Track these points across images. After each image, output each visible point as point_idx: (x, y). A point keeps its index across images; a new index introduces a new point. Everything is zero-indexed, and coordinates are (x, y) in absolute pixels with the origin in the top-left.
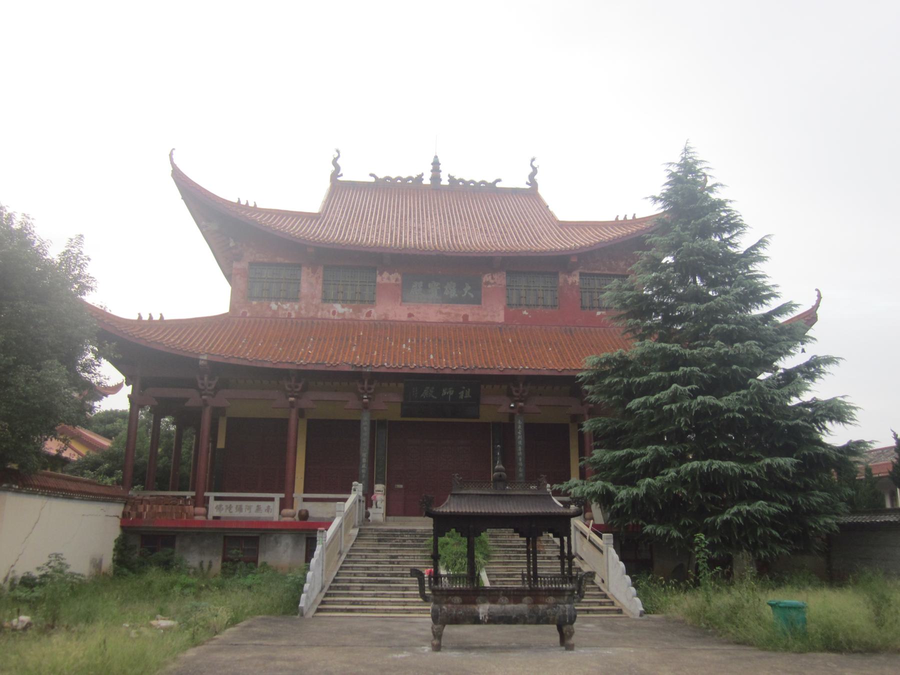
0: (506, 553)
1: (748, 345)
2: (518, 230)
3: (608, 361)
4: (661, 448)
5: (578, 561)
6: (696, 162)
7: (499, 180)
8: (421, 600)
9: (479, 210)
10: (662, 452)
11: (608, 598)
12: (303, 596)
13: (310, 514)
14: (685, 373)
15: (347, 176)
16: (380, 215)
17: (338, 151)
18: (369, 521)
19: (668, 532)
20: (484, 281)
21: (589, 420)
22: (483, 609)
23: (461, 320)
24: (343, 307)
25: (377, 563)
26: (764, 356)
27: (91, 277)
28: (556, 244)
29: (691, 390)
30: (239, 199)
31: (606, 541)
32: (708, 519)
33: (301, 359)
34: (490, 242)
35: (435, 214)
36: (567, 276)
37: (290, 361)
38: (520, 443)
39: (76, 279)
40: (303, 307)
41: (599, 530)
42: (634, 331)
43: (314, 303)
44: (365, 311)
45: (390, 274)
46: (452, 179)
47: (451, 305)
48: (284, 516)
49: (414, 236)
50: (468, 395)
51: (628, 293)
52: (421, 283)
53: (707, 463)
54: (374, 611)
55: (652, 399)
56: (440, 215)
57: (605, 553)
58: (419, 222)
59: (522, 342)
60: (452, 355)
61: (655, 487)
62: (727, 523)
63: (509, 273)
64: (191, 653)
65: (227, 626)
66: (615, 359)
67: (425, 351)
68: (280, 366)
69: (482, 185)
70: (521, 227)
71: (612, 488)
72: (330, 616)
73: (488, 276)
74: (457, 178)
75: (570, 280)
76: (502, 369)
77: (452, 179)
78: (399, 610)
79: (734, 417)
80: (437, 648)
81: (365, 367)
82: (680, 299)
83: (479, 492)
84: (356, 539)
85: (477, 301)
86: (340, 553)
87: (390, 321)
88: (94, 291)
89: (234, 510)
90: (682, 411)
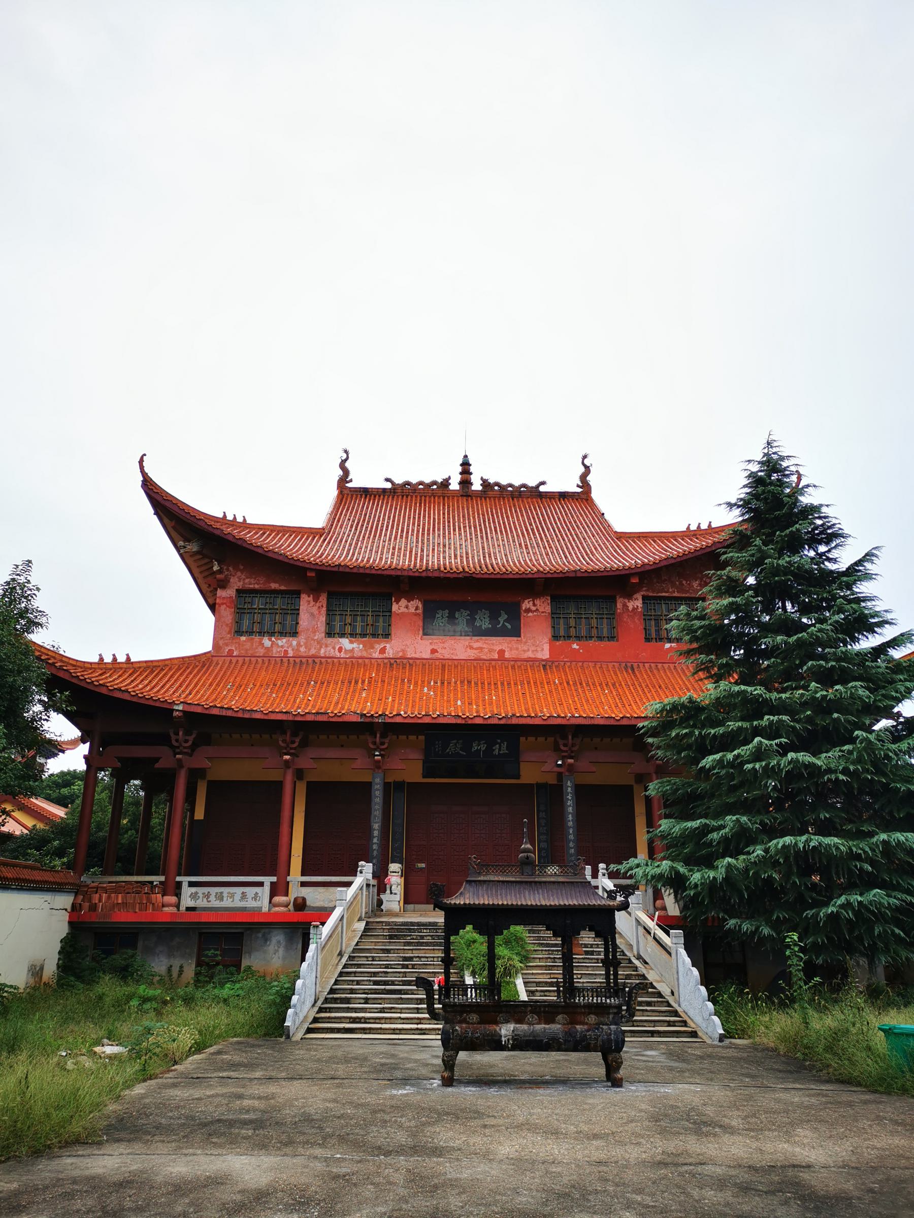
0: (549, 954)
1: (852, 687)
2: (566, 544)
3: (675, 708)
4: (744, 819)
5: (641, 966)
6: (782, 458)
7: (543, 483)
8: (427, 1016)
9: (518, 520)
10: (746, 824)
11: (680, 1016)
12: (290, 1011)
13: (309, 903)
14: (771, 723)
15: (358, 481)
16: (397, 529)
17: (346, 452)
18: (382, 910)
19: (757, 928)
20: (524, 608)
21: (656, 782)
22: (506, 1030)
23: (496, 656)
24: (351, 642)
25: (387, 967)
26: (875, 701)
27: (40, 611)
28: (612, 561)
29: (779, 745)
30: (224, 513)
31: (674, 940)
32: (808, 912)
33: (299, 708)
34: (531, 560)
35: (465, 527)
36: (626, 601)
37: (284, 711)
38: (570, 809)
39: (23, 613)
40: (302, 644)
41: (667, 924)
42: (707, 669)
43: (316, 638)
44: (379, 647)
45: (409, 601)
46: (485, 483)
47: (484, 638)
48: (275, 906)
49: (439, 554)
50: (504, 750)
51: (697, 623)
52: (447, 611)
53: (804, 838)
54: (380, 1031)
55: (730, 756)
56: (470, 528)
57: (673, 955)
58: (444, 537)
59: (571, 683)
60: (484, 701)
61: (737, 869)
62: (833, 917)
63: (554, 599)
64: (139, 1089)
65: (190, 1053)
66: (683, 706)
67: (452, 695)
68: (273, 717)
69: (522, 489)
70: (569, 540)
71: (682, 869)
72: (323, 1038)
73: (529, 602)
74: (491, 481)
75: (631, 605)
76: (546, 718)
77: (485, 483)
78: (411, 1029)
79: (837, 779)
80: (448, 1082)
81: (376, 717)
82: (766, 629)
83: (501, 879)
84: (362, 935)
85: (516, 632)
86: (341, 954)
87: (411, 659)
88: (44, 628)
89: (212, 898)
90: (769, 772)
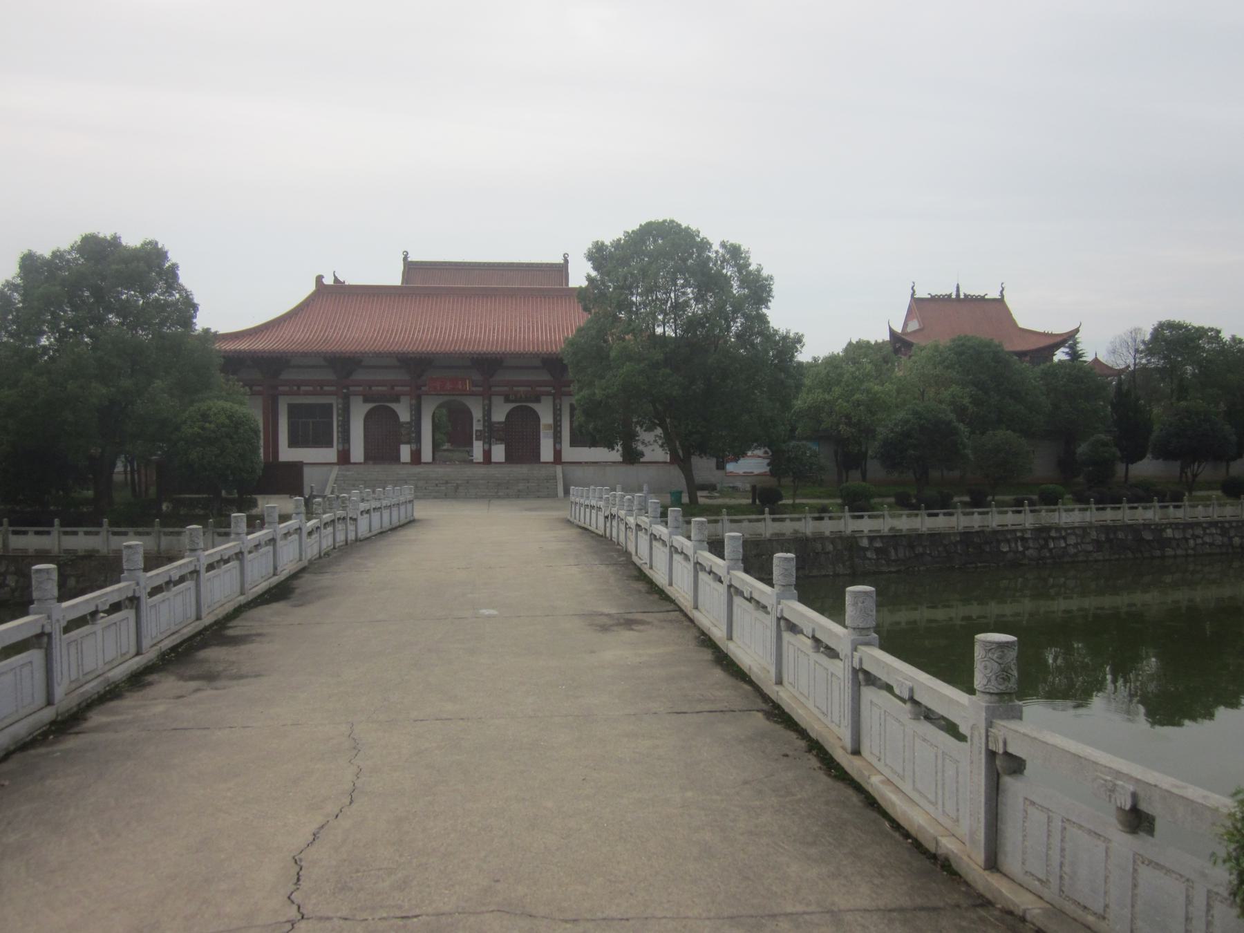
7: (986, 295)
17: (914, 283)
46: (965, 295)
77: (965, 295)
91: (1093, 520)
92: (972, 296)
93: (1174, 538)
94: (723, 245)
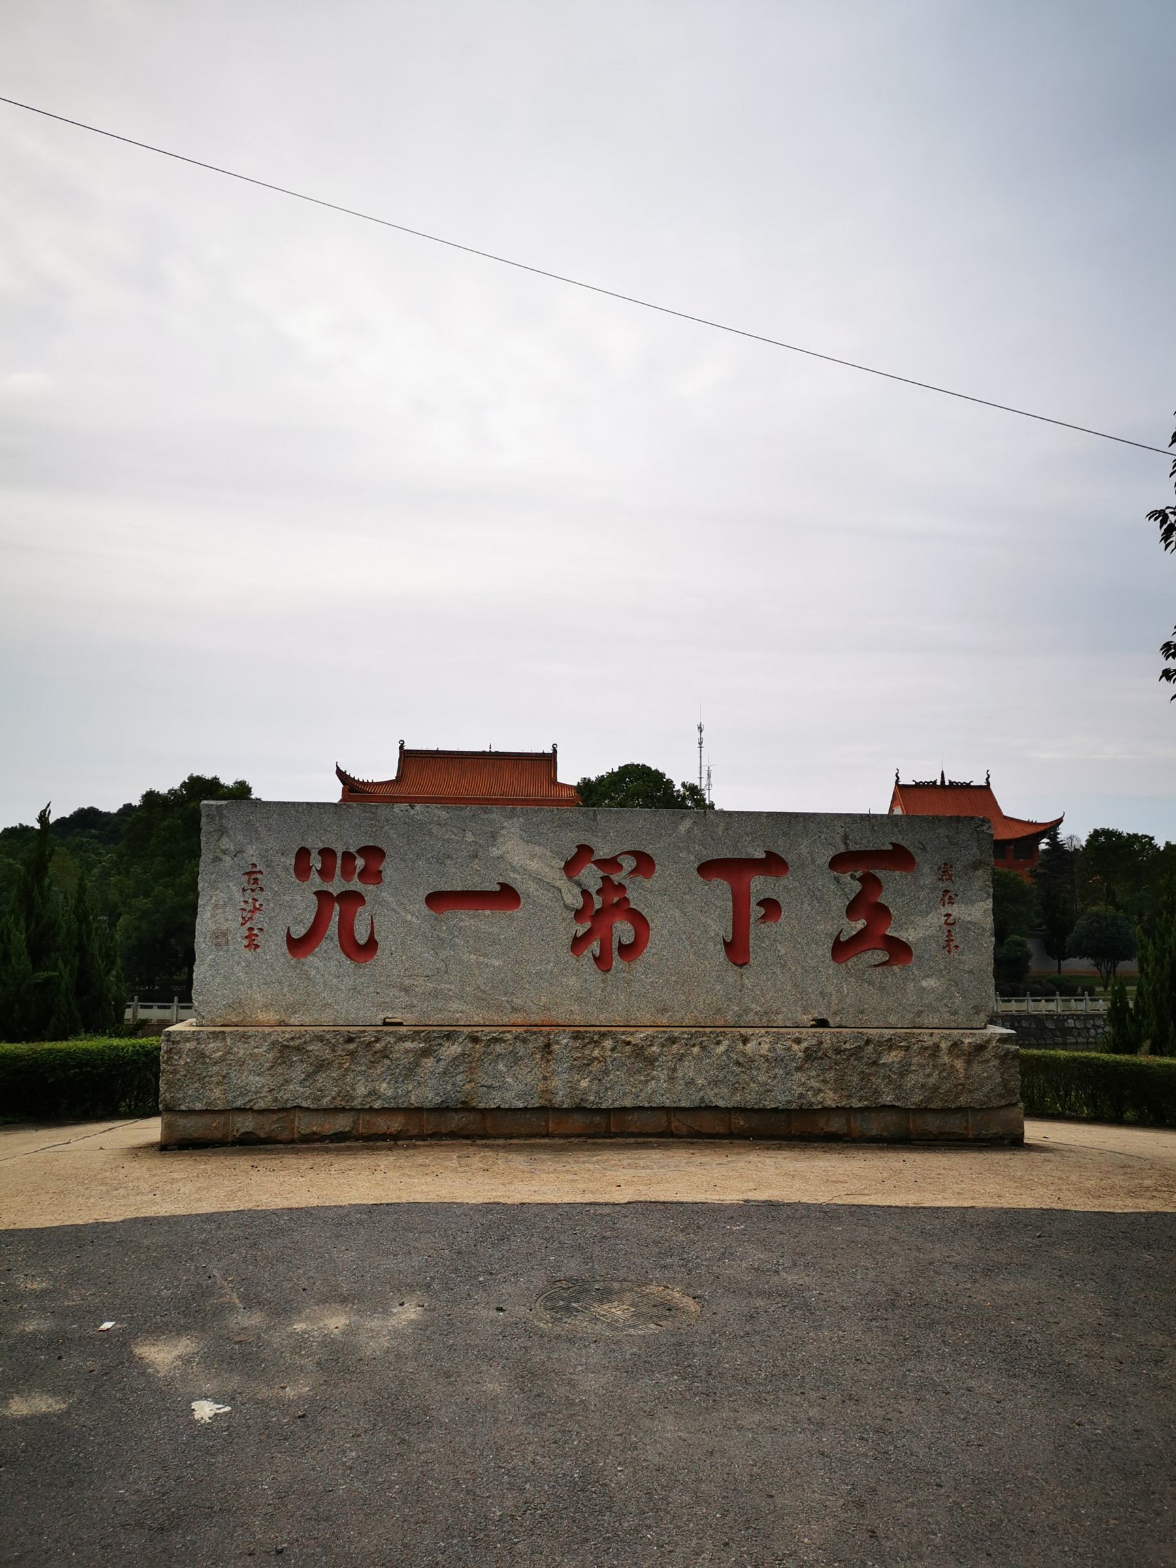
46: (950, 782)
77: (950, 782)
91: (999, 1011)
92: (957, 783)
93: (1075, 1028)
94: (684, 785)
